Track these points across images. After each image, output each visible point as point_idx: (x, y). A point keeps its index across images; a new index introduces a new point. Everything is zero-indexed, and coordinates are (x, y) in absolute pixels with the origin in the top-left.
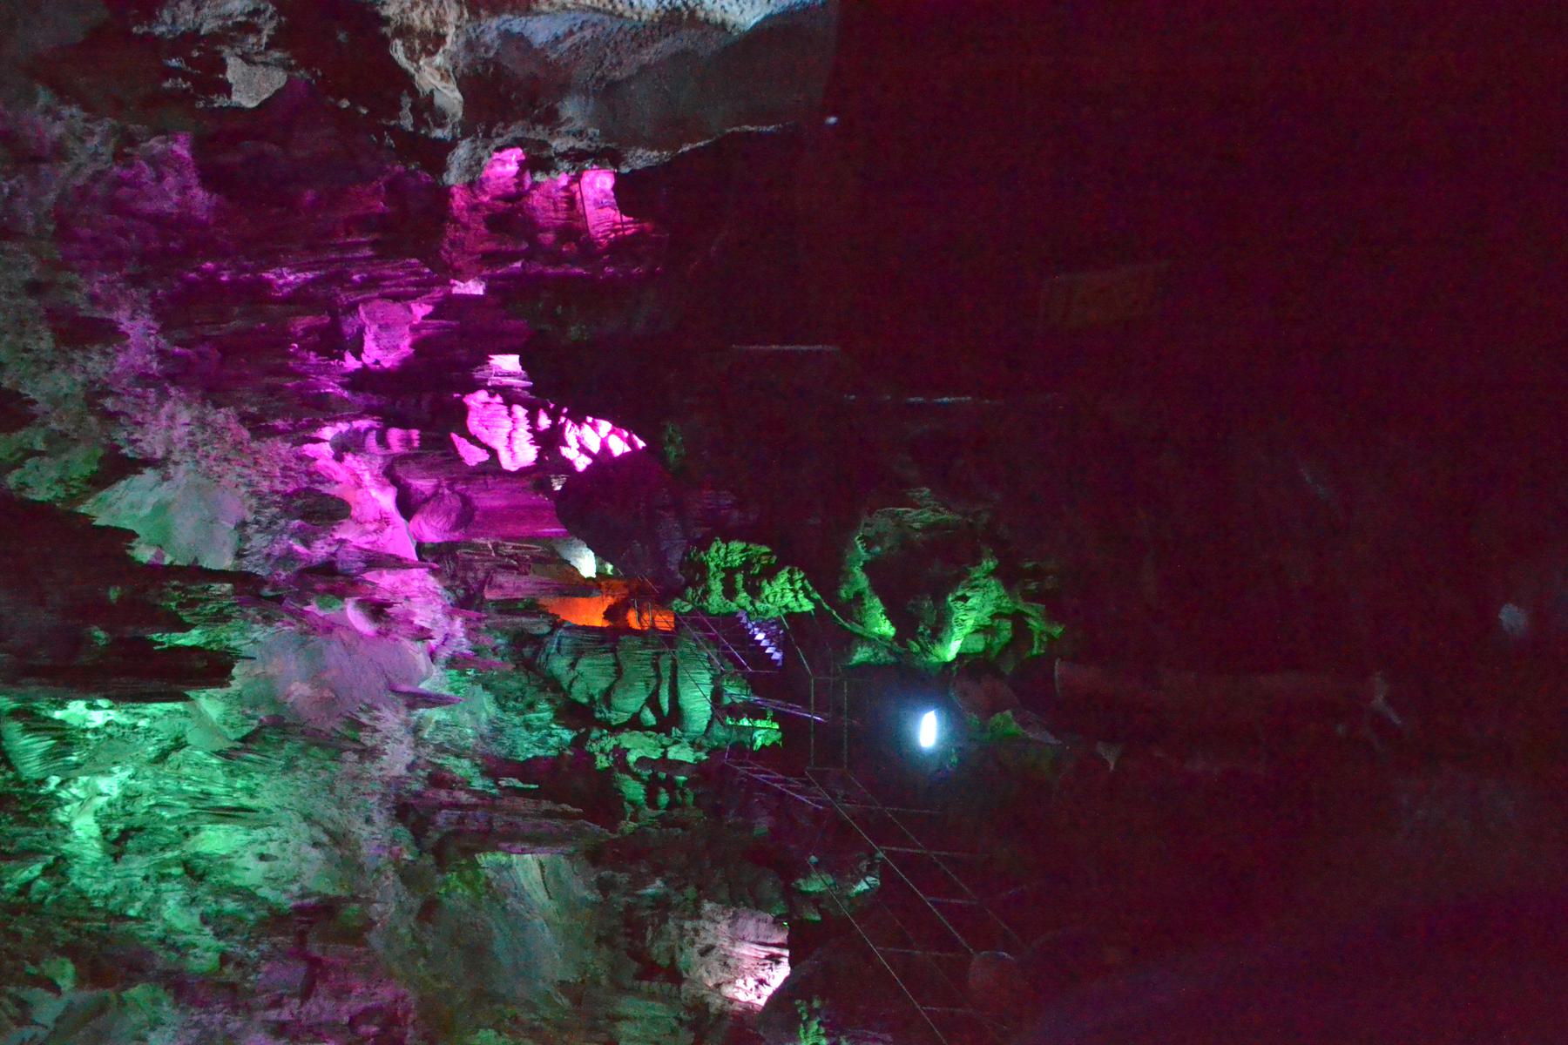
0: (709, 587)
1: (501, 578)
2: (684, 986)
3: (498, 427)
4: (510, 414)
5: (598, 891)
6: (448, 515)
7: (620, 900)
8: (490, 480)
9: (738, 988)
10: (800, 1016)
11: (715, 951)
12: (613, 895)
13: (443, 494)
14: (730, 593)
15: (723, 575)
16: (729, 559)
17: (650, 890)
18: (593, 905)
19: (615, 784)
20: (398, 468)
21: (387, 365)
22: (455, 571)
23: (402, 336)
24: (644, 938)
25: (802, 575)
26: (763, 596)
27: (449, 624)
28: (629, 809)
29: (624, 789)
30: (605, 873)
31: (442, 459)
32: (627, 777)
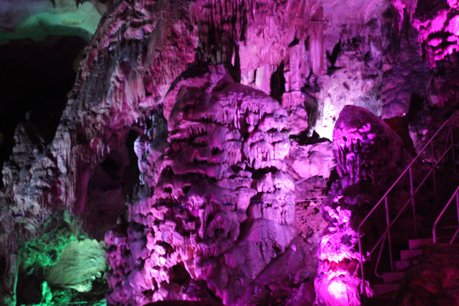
2: (327, 77)
5: (369, 20)
7: (365, 33)
9: (329, 107)
10: (361, 127)
11: (346, 90)
12: (368, 29)
17: (373, 50)
18: (362, 19)
19: (439, 12)
24: (349, 50)
28: (425, 24)
29: (437, 18)
30: (379, 23)
32: (445, 18)
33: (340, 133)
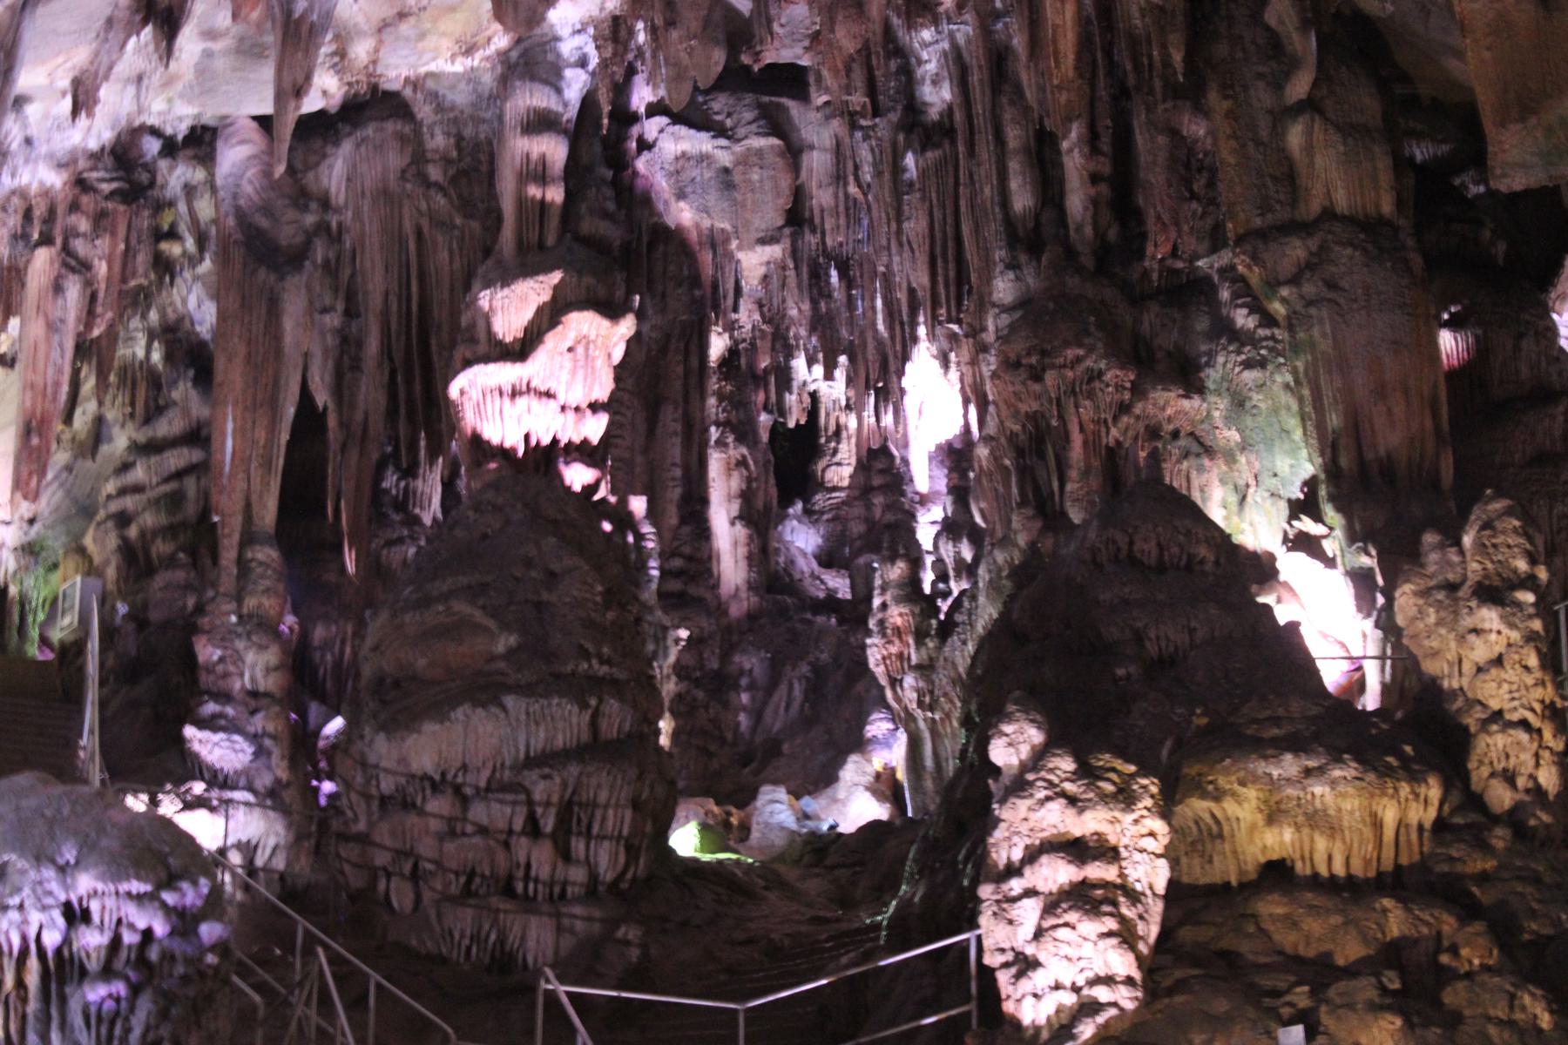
0: (1093, 808)
1: (74, 291)
3: (573, 372)
4: (595, 407)
6: (266, 209)
8: (333, 320)
13: (305, 208)
14: (1077, 849)
15: (1113, 840)
16: (1137, 856)
20: (391, 126)
21: (641, 164)
22: (95, 191)
23: (704, 210)
25: (1129, 1005)
26: (1072, 917)
27: (50, 156)
31: (408, 227)
33: (54, 886)
